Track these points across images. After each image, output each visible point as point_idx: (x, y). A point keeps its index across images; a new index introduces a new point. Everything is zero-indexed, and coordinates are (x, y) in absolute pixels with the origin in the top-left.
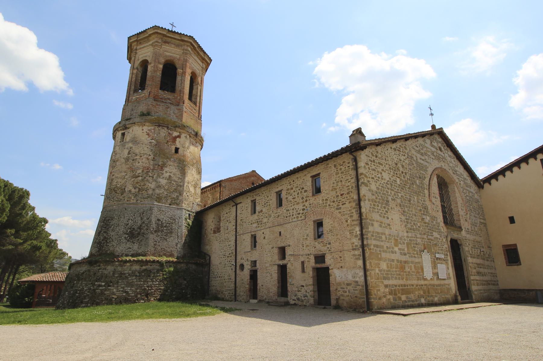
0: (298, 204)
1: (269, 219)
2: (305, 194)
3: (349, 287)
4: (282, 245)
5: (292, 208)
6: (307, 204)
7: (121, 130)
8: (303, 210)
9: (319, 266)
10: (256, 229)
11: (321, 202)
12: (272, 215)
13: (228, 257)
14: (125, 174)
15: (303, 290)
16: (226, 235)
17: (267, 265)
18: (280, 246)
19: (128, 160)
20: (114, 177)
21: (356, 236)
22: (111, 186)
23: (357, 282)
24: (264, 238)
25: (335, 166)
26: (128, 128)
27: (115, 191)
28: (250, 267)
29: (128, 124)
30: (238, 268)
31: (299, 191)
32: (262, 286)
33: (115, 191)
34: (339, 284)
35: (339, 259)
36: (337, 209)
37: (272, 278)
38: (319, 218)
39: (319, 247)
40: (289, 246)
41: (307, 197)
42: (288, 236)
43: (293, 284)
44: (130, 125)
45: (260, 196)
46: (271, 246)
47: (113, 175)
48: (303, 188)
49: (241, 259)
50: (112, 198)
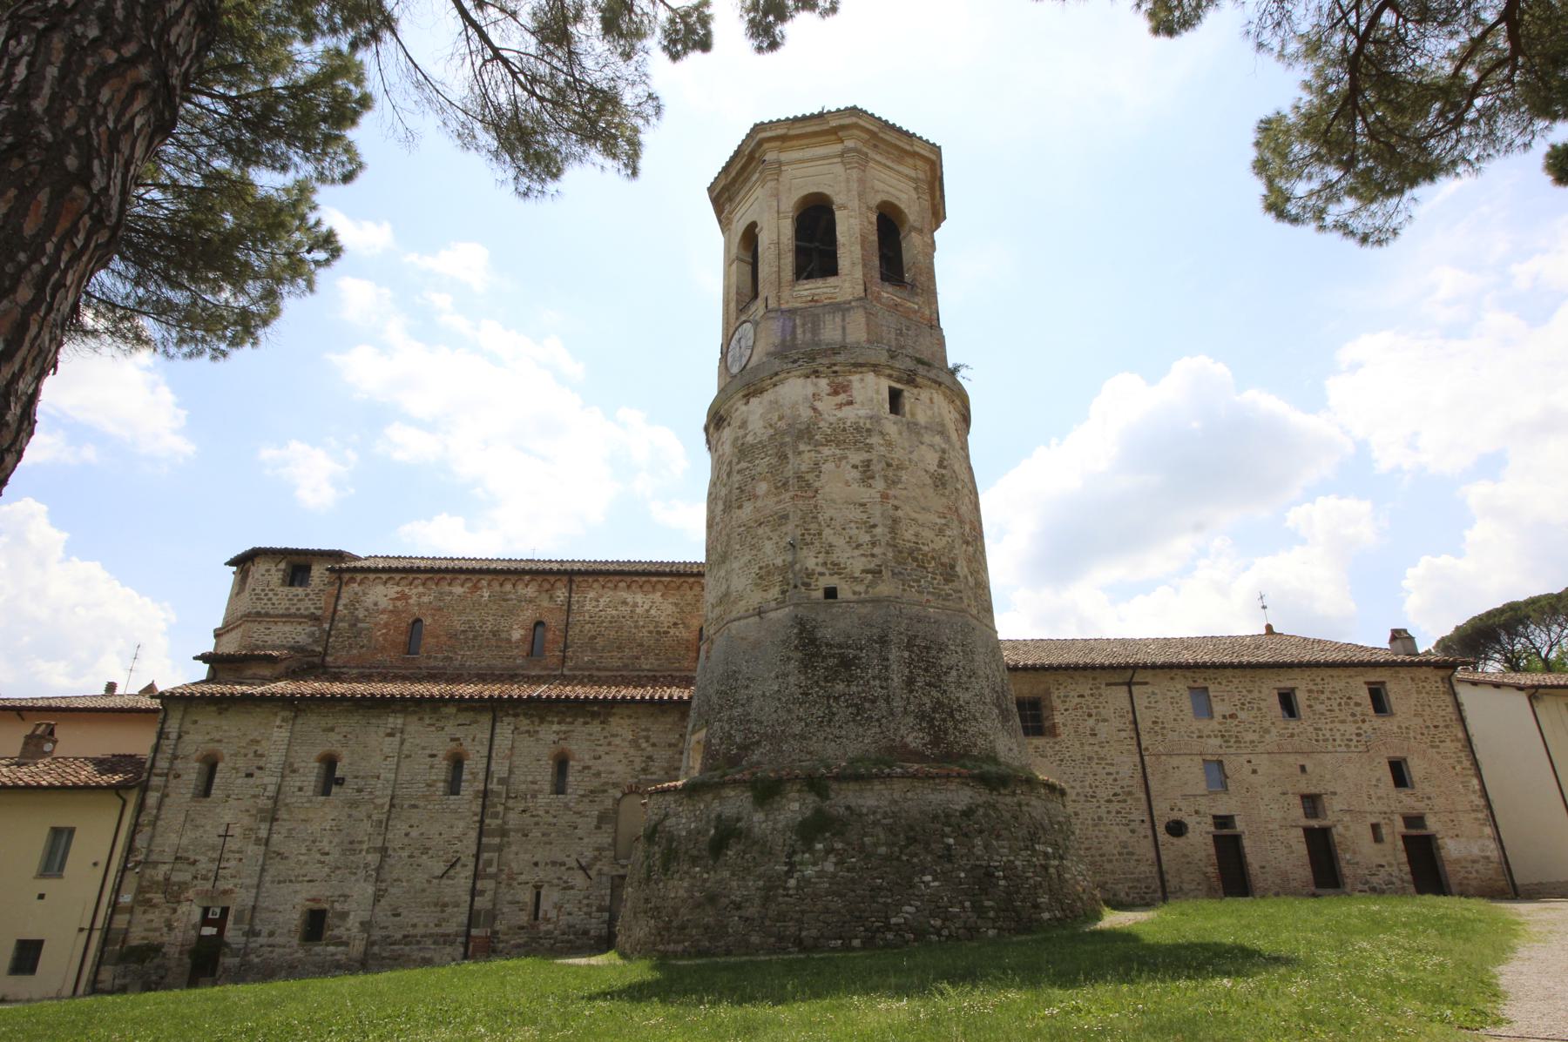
0: (1343, 722)
1: (1261, 737)
2: (1359, 709)
3: (1476, 866)
4: (1313, 790)
5: (1328, 727)
6: (1365, 726)
7: (890, 376)
8: (1358, 735)
9: (1414, 832)
10: (1220, 751)
11: (1395, 729)
12: (1274, 731)
13: (1109, 801)
14: (943, 521)
15: (1382, 873)
16: (1087, 748)
17: (1275, 826)
18: (1307, 791)
19: (944, 485)
20: (900, 513)
21: (1474, 792)
22: (894, 538)
23: (1487, 858)
24: (1254, 772)
25: (1412, 679)
26: (916, 387)
27: (915, 560)
28: (1212, 829)
29: (924, 377)
30: (1161, 829)
31: (1343, 702)
32: (1263, 867)
33: (915, 560)
34: (1457, 861)
35: (1451, 824)
36: (1432, 747)
37: (1292, 852)
38: (1398, 754)
39: (1407, 801)
40: (1334, 793)
41: (1363, 715)
42: (1328, 777)
43: (1357, 863)
44: (926, 382)
45: (1220, 683)
46: (1279, 790)
47: (896, 508)
48: (1349, 698)
49: (1172, 809)
50: (914, 581)
